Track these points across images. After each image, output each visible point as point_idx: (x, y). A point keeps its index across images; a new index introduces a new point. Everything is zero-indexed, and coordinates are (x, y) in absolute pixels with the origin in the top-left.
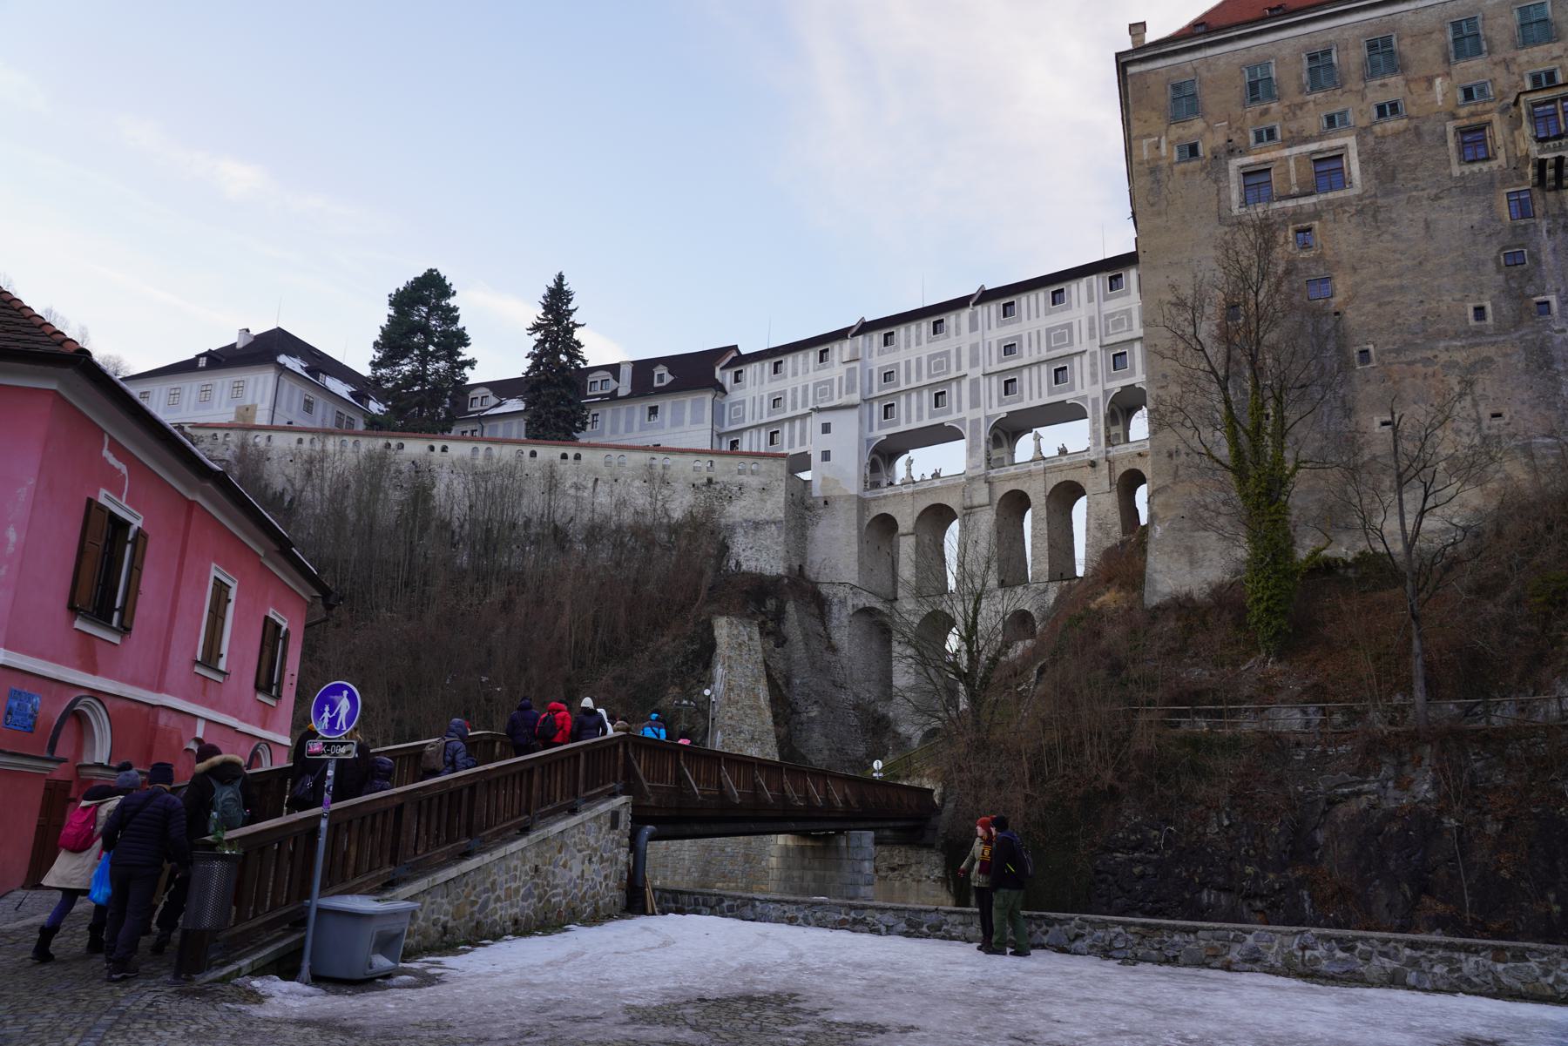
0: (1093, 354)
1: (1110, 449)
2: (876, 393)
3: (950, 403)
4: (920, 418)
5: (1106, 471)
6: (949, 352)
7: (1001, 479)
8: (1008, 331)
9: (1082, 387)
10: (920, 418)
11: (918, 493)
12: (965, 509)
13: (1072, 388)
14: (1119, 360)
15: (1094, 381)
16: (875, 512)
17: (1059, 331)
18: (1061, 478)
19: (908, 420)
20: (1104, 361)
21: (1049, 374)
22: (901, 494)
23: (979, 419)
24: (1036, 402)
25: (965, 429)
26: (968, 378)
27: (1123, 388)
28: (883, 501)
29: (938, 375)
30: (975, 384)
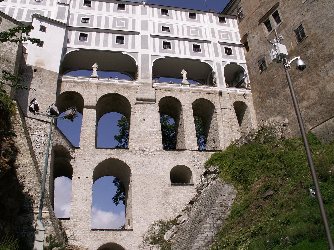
0: (215, 44)
1: (228, 89)
2: (75, 24)
3: (127, 44)
4: (105, 44)
5: (228, 98)
6: (127, 20)
7: (162, 89)
8: (165, 21)
9: (210, 56)
10: (105, 44)
11: (100, 84)
12: (138, 100)
14: (228, 51)
15: (217, 55)
18: (200, 96)
19: (97, 43)
20: (221, 49)
21: (190, 45)
23: (147, 56)
24: (182, 56)
25: (137, 59)
27: (231, 63)
28: (74, 84)
29: (120, 28)
30: (144, 39)
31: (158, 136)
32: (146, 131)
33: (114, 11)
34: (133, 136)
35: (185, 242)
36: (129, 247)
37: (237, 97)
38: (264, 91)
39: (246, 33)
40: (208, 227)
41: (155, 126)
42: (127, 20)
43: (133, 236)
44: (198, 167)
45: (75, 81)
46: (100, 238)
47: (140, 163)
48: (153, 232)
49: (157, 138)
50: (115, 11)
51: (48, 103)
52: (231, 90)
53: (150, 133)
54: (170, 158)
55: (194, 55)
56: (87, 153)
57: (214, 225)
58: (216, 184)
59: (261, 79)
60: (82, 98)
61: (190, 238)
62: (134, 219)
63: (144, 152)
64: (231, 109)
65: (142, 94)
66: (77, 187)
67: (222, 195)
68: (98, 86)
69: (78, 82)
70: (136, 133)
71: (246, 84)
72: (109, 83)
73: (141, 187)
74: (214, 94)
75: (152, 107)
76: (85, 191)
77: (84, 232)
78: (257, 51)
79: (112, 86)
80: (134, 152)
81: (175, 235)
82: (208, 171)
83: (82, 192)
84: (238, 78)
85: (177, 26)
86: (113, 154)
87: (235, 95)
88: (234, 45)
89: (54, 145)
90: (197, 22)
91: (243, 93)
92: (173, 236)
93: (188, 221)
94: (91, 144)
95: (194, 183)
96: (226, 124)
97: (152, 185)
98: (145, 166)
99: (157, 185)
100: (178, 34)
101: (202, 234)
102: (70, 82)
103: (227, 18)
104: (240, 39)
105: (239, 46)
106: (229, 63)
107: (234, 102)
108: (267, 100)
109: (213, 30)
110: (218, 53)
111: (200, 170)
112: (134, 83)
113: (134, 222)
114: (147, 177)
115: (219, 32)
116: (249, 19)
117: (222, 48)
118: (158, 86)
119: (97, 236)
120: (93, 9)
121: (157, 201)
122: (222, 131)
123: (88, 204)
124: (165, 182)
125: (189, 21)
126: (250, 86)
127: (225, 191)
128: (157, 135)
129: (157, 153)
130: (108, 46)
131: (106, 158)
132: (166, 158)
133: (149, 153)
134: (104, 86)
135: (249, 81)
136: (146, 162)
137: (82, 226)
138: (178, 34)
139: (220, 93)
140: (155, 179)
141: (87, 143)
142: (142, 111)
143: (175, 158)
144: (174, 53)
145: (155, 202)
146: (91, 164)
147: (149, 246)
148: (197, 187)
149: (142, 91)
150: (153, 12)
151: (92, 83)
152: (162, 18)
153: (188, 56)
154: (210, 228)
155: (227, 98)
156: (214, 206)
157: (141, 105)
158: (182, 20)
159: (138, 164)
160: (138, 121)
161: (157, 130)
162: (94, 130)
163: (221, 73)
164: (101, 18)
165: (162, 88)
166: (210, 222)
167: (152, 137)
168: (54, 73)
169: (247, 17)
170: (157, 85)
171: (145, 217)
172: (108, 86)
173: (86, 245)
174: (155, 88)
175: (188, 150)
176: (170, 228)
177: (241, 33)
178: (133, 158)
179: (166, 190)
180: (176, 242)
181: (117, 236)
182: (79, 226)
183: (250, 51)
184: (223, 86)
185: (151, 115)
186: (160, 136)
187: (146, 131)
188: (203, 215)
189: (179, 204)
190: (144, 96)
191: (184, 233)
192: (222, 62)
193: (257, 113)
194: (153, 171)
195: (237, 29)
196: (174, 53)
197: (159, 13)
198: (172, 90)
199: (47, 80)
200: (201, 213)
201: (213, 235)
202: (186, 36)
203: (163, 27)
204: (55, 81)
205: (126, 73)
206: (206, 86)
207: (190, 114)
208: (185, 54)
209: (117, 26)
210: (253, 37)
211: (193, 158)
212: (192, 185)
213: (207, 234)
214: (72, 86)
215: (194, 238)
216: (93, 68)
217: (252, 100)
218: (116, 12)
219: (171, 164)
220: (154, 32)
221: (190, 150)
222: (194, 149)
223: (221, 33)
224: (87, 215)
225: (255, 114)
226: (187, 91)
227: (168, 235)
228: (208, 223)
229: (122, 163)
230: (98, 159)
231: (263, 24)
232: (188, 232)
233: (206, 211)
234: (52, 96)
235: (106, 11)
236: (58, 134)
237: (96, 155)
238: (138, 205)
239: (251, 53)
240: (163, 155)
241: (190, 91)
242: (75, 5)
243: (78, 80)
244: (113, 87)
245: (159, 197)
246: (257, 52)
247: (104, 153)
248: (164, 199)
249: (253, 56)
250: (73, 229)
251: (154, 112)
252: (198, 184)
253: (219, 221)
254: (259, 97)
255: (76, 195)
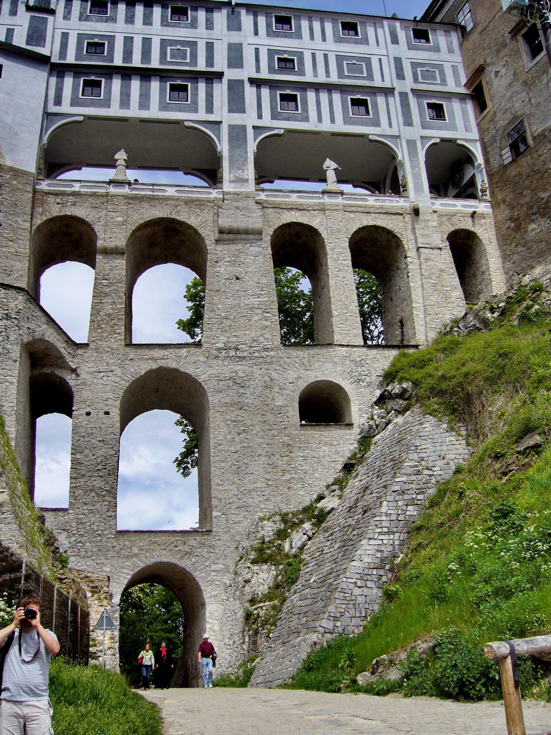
0: (403, 95)
1: (434, 201)
2: (71, 59)
3: (195, 102)
4: (144, 103)
6: (195, 43)
7: (277, 207)
11: (134, 198)
12: (221, 232)
13: (377, 123)
15: (408, 122)
16: (55, 211)
17: (354, 62)
21: (343, 102)
22: (107, 195)
23: (244, 128)
24: (326, 126)
26: (225, 80)
27: (443, 140)
31: (270, 315)
32: (243, 304)
33: (162, 25)
34: (212, 315)
35: (331, 559)
36: (204, 571)
37: (455, 220)
38: (522, 202)
39: (478, 66)
40: (384, 524)
41: (263, 292)
42: (193, 45)
43: (214, 545)
44: (363, 384)
45: (74, 192)
46: (137, 551)
47: (227, 378)
48: (259, 536)
49: (267, 320)
50: (165, 23)
51: (11, 243)
52: (441, 205)
53: (251, 309)
54: (297, 365)
55: (353, 124)
56: (105, 358)
57: (398, 517)
58: (405, 423)
59: (515, 175)
60: (93, 230)
61: (342, 550)
62: (216, 507)
63: (238, 352)
64: (440, 249)
65: (231, 217)
66: (83, 434)
67: (418, 448)
68: (130, 201)
69: (83, 193)
70: (218, 308)
71: (479, 188)
72: (155, 194)
73: (230, 432)
74: (401, 214)
75: (254, 249)
76: (101, 444)
77: (99, 538)
78: (506, 107)
79: (161, 201)
80: (215, 352)
81: (309, 542)
82: (386, 393)
83: (94, 448)
84: (460, 176)
85: (313, 55)
86: (165, 357)
87: (451, 216)
88: (449, 96)
89: (26, 339)
90: (362, 43)
91: (472, 210)
92: (304, 545)
93: (339, 510)
94: (116, 335)
95: (353, 422)
96: (429, 285)
97: (256, 427)
98: (240, 384)
99: (269, 428)
100: (316, 76)
101: (370, 539)
102: (63, 194)
103: (434, 30)
104: (464, 80)
105: (462, 97)
106: (438, 141)
107: (448, 233)
108: (529, 224)
109: (398, 61)
110: (410, 117)
111: (367, 391)
112: (214, 194)
113: (215, 513)
114: (245, 410)
115: (414, 65)
116: (488, 29)
117: (420, 105)
118: (269, 199)
119: (131, 548)
120: (113, 20)
121: (269, 464)
122: (421, 301)
123: (109, 474)
124: (288, 419)
125: (341, 42)
126: (488, 193)
127: (425, 438)
128: (267, 312)
129: (267, 354)
130: (151, 108)
131: (149, 368)
132: (288, 364)
133: (250, 353)
134: (144, 201)
135: (486, 181)
136: (242, 375)
137: (96, 524)
138: (316, 76)
139: (416, 212)
140: (264, 413)
141: (105, 335)
142: (233, 258)
143: (311, 365)
144: (306, 119)
145: (264, 466)
146: (115, 383)
147: (249, 568)
148: (361, 432)
149: (232, 212)
150: (256, 24)
151: (115, 196)
152: (277, 36)
153: (340, 127)
154: (388, 525)
155: (431, 224)
156: (398, 475)
157: (229, 244)
158: (324, 40)
159: (224, 379)
160: (223, 281)
161: (266, 301)
162: (122, 303)
163: (419, 164)
164: (132, 42)
165: (279, 204)
166: (389, 512)
167: (256, 318)
168: (25, 173)
169: (481, 24)
170: (267, 197)
171: (241, 501)
172: (152, 203)
173: (105, 569)
174: (261, 203)
175: (340, 345)
176: (295, 526)
177: (466, 67)
178: (212, 367)
179: (289, 438)
180: (310, 558)
181: (176, 547)
182: (88, 524)
183: (488, 109)
184: (423, 195)
185: (253, 267)
186: (274, 316)
187: (243, 304)
188: (374, 495)
189: (320, 470)
190: (235, 222)
191: (330, 538)
192: (421, 137)
193: (505, 257)
194: (258, 396)
195: (457, 58)
196: (306, 119)
197: (269, 26)
198: (300, 208)
199: (8, 189)
200: (369, 491)
201: (397, 543)
202: (334, 78)
203: (279, 60)
204: (26, 191)
205: (199, 174)
206: (382, 195)
207: (345, 262)
208: (333, 121)
209: (171, 58)
210: (497, 73)
211: (352, 365)
212: (350, 425)
213: (382, 540)
214: (69, 204)
215: (351, 548)
216: (117, 160)
217: (493, 226)
218: (167, 26)
219: (300, 378)
220: (258, 70)
221: (343, 346)
222: (353, 344)
223: (419, 69)
224: (106, 498)
225: (500, 260)
226: (337, 208)
227: (294, 544)
228: (384, 514)
229: (187, 378)
230: (132, 370)
231: (520, 38)
232: (339, 534)
233: (381, 485)
234: (21, 227)
235: (144, 24)
236: (35, 315)
237: (128, 362)
238: (223, 473)
239: (492, 113)
240: (281, 357)
241: (346, 209)
242: (70, 13)
243: (82, 190)
244: (165, 203)
245: (273, 455)
246: (507, 109)
247: (145, 357)
248: (285, 459)
249: (495, 120)
250: (74, 532)
251: (260, 259)
252: (363, 424)
253: (410, 508)
254: (510, 219)
255: (81, 453)
